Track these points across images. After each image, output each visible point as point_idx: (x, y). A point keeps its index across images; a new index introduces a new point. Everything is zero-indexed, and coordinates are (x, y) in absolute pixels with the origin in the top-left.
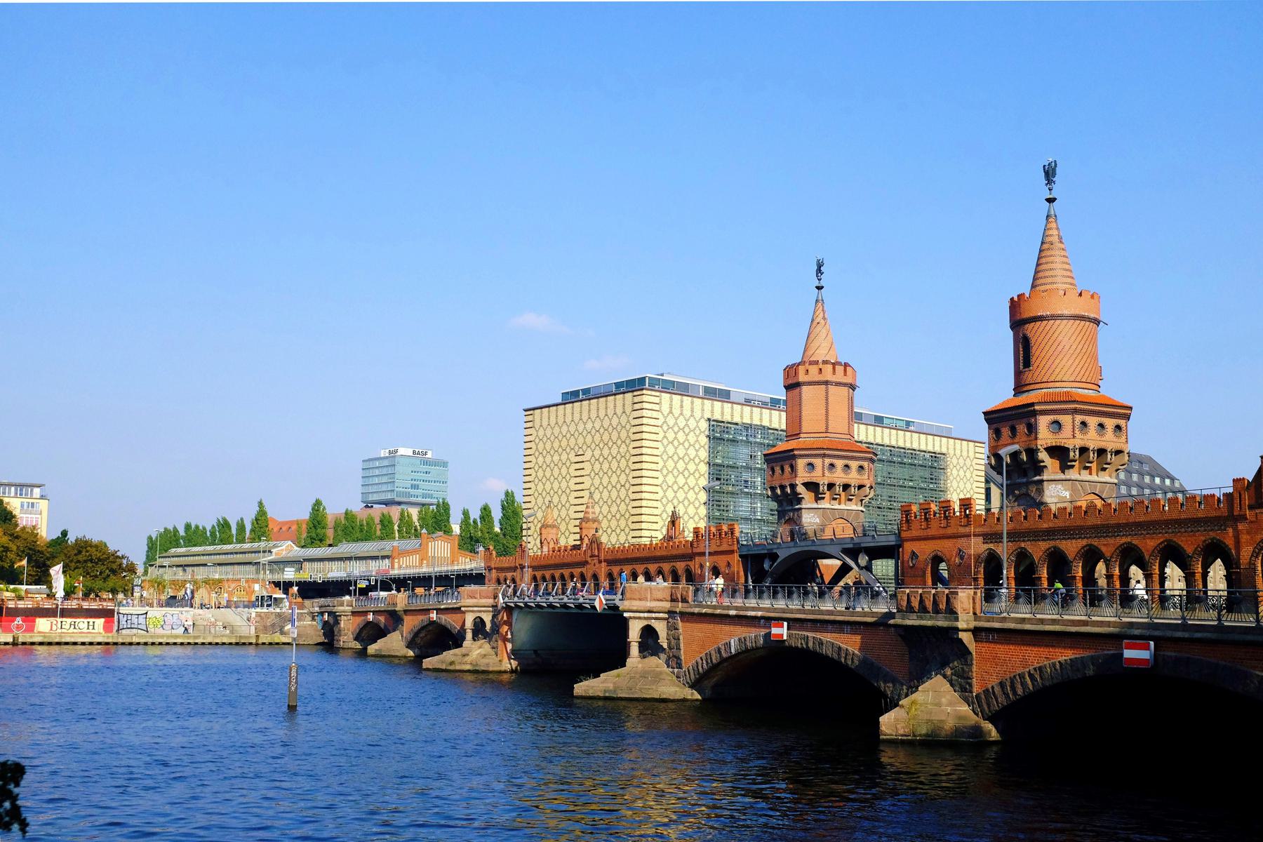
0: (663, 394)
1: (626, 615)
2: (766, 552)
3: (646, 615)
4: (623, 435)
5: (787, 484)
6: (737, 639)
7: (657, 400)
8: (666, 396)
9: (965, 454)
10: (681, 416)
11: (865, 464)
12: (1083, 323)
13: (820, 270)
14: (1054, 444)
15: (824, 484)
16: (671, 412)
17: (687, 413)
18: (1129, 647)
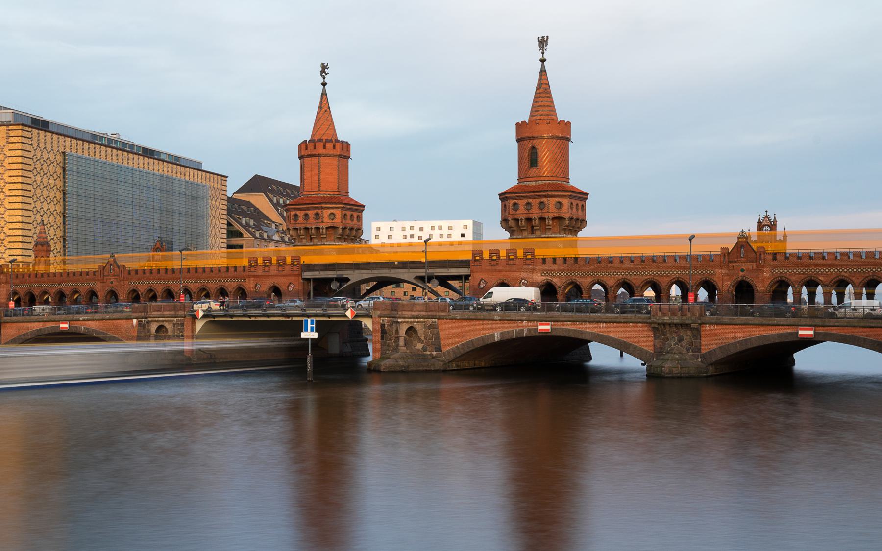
0: (33, 130)
1: (399, 320)
2: (335, 276)
3: (412, 320)
5: (313, 227)
6: (499, 333)
7: (28, 135)
8: (35, 131)
9: (216, 186)
10: (45, 150)
13: (324, 72)
14: (558, 216)
15: (323, 228)
16: (38, 146)
17: (49, 147)
18: (801, 329)
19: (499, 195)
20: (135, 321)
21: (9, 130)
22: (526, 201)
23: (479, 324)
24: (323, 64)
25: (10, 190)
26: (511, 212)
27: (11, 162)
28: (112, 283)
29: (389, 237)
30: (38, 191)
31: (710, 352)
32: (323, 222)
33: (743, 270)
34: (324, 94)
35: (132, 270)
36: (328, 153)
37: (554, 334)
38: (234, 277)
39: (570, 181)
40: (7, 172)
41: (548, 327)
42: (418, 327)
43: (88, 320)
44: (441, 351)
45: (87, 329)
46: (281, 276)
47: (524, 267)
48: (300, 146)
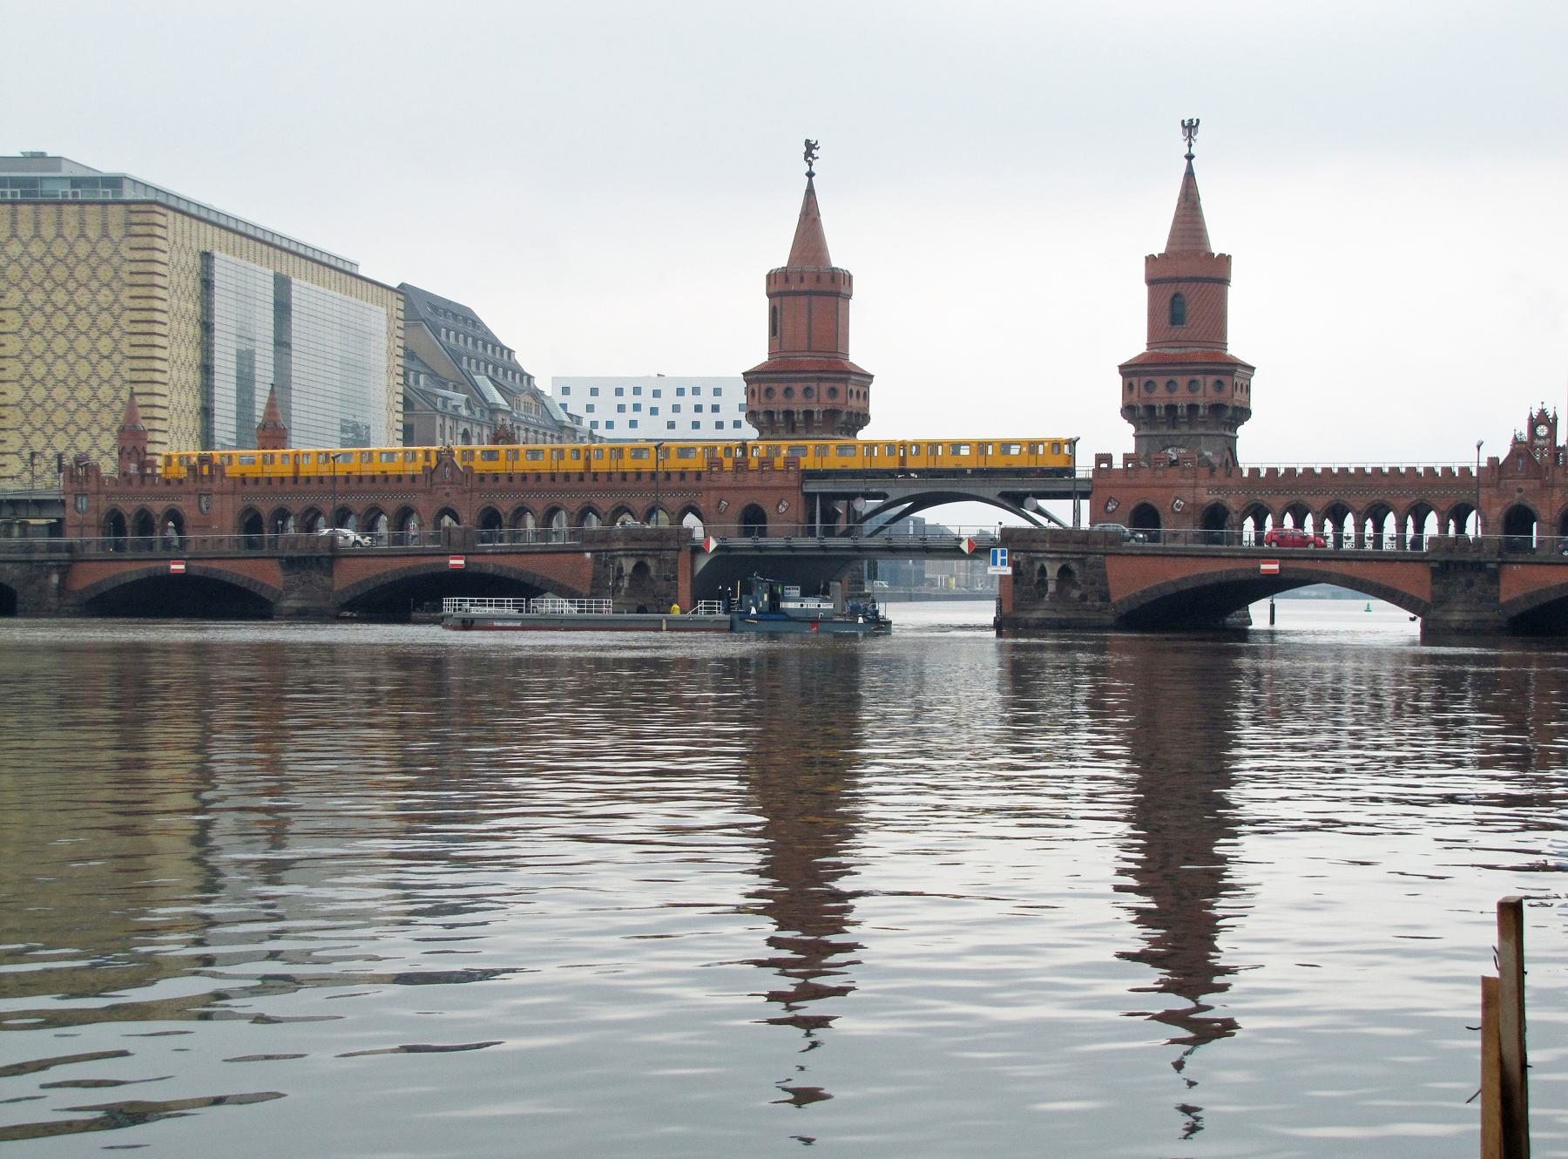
2: (863, 490)
4: (105, 273)
5: (801, 410)
8: (171, 214)
11: (814, 385)
12: (1212, 285)
13: (812, 156)
16: (175, 242)
19: (1121, 367)
20: (588, 555)
21: (132, 212)
22: (1167, 379)
23: (1169, 562)
24: (807, 142)
25: (132, 322)
26: (1144, 394)
27: (134, 270)
28: (447, 495)
29: (590, 408)
30: (175, 324)
31: (1511, 603)
32: (818, 400)
33: (1520, 490)
34: (810, 192)
35: (488, 475)
36: (825, 289)
37: (1284, 575)
38: (679, 489)
39: (1228, 347)
40: (126, 288)
41: (1276, 567)
42: (1074, 566)
43: (501, 554)
44: (1110, 601)
45: (501, 567)
46: (766, 488)
47: (1182, 481)
48: (769, 276)
